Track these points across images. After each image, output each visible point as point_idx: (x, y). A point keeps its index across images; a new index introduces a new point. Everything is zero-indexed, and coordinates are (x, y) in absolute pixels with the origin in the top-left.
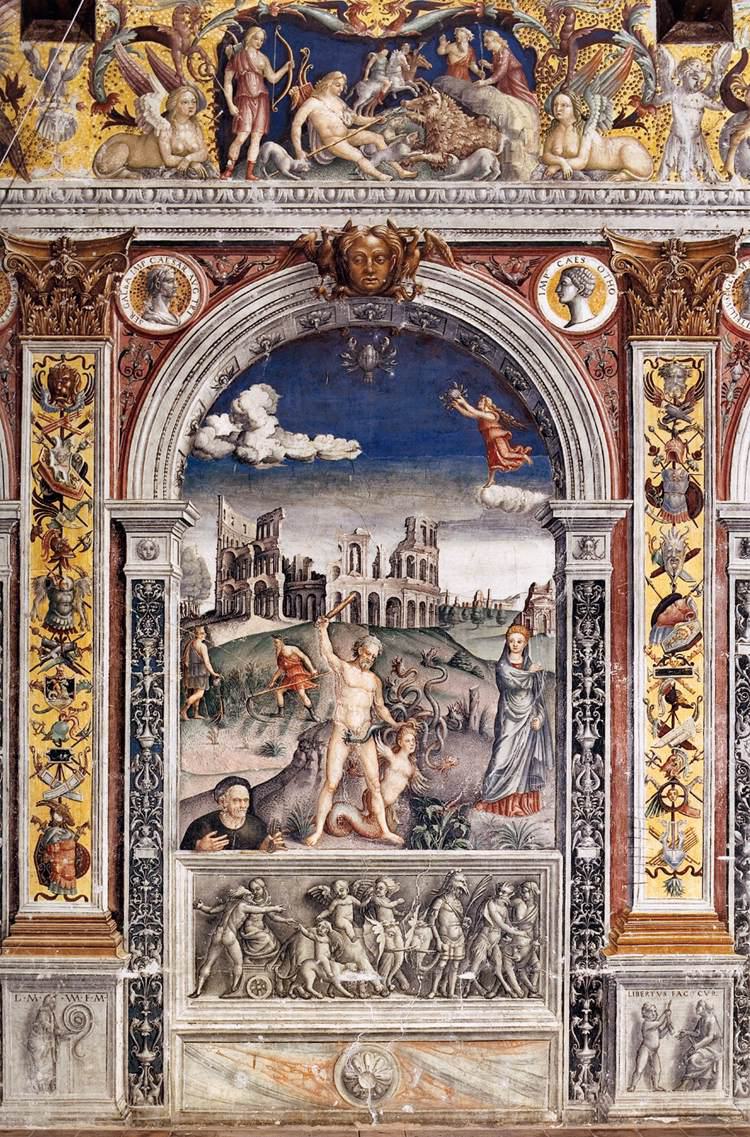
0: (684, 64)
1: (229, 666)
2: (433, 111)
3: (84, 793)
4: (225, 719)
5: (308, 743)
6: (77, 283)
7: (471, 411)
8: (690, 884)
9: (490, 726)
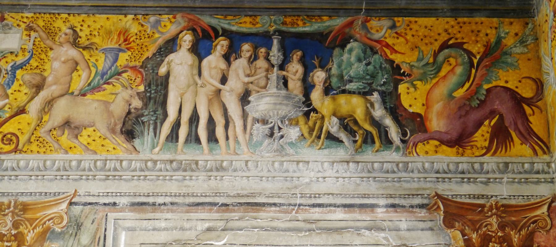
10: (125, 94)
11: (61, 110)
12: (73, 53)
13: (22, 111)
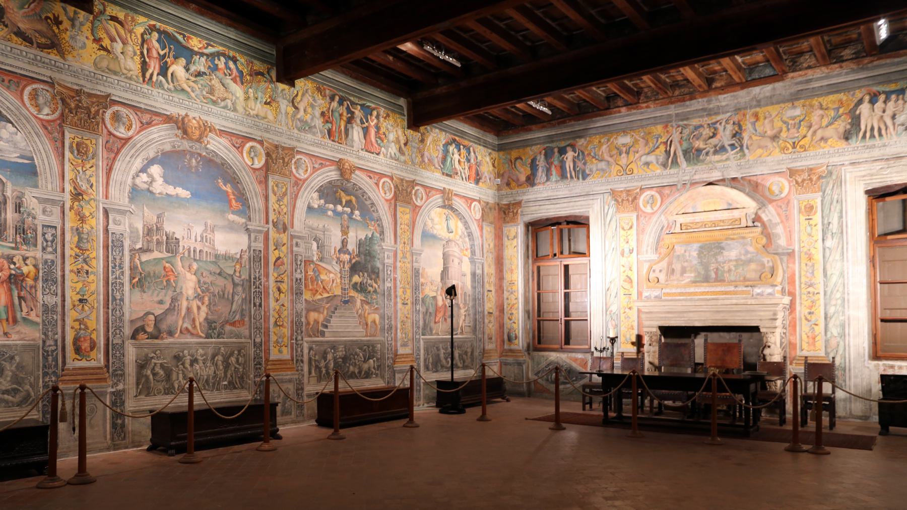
0: (283, 90)
1: (147, 269)
2: (213, 82)
3: (93, 316)
4: (146, 290)
5: (174, 300)
6: (88, 109)
7: (224, 188)
8: (284, 350)
9: (230, 296)
10: (844, 124)
11: (820, 134)
12: (821, 112)
13: (805, 137)
